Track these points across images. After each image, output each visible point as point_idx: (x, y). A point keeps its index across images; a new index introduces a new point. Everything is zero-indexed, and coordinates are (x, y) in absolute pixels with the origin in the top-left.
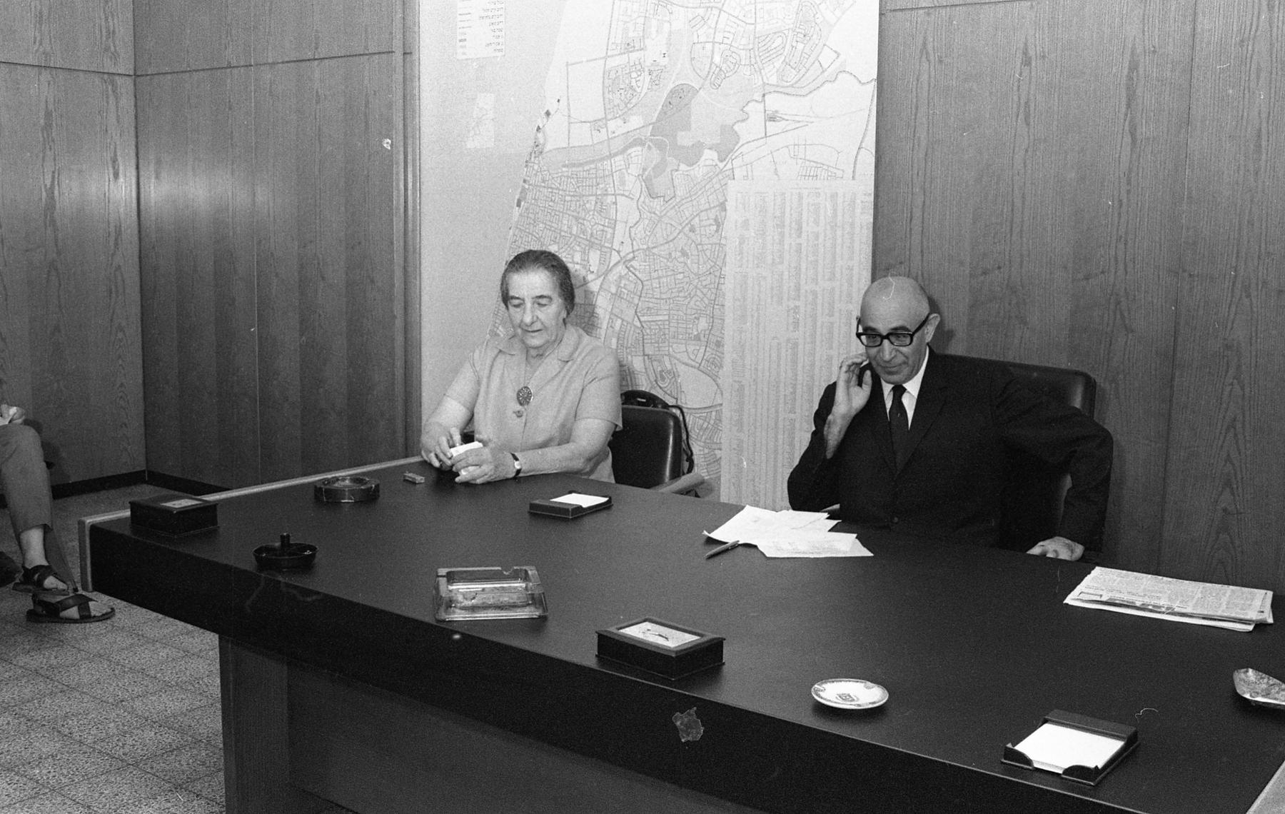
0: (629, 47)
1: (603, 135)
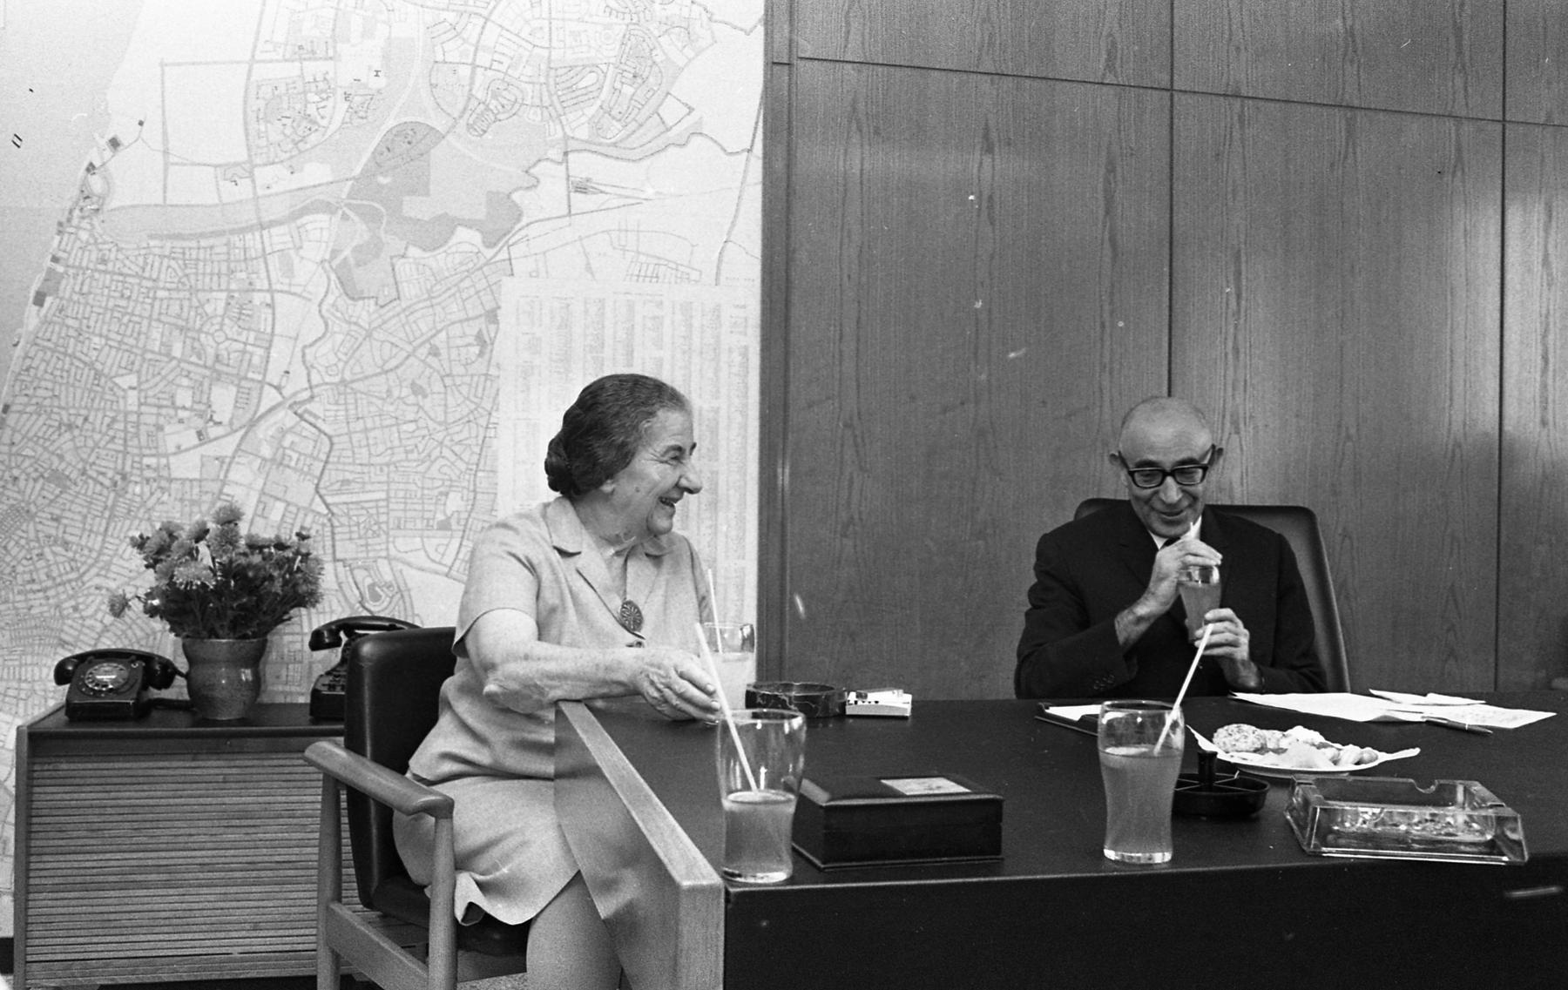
0: (303, 52)
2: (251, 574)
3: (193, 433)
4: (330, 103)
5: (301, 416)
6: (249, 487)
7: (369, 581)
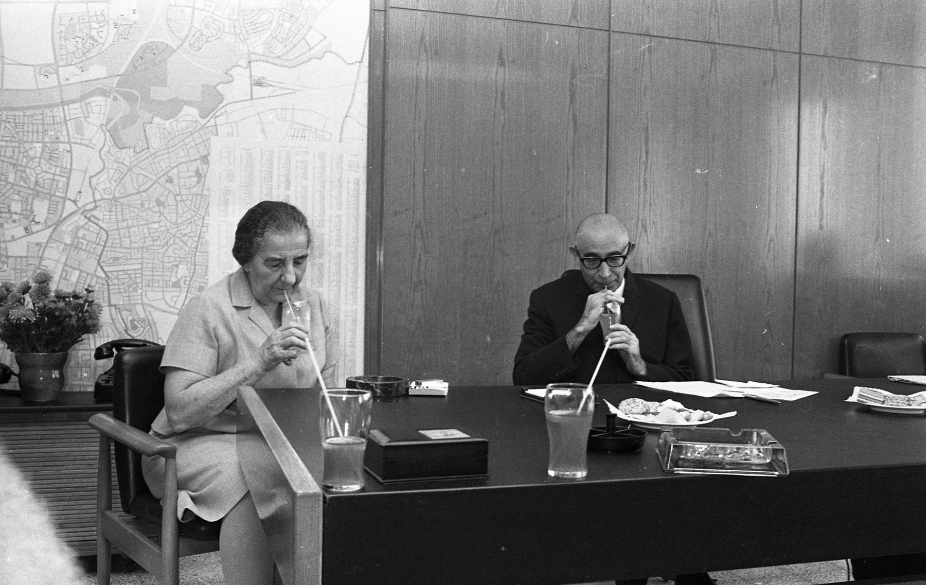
1: (52, 81)
2: (57, 313)
3: (21, 229)
4: (105, 29)
5: (89, 219)
6: (57, 261)
7: (130, 318)
